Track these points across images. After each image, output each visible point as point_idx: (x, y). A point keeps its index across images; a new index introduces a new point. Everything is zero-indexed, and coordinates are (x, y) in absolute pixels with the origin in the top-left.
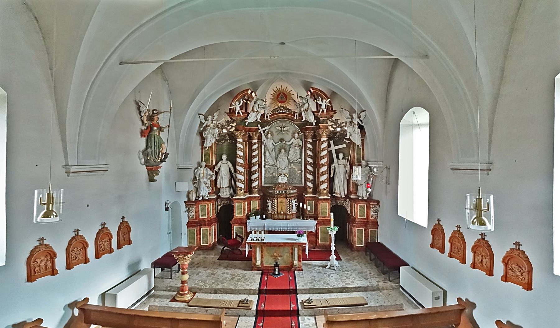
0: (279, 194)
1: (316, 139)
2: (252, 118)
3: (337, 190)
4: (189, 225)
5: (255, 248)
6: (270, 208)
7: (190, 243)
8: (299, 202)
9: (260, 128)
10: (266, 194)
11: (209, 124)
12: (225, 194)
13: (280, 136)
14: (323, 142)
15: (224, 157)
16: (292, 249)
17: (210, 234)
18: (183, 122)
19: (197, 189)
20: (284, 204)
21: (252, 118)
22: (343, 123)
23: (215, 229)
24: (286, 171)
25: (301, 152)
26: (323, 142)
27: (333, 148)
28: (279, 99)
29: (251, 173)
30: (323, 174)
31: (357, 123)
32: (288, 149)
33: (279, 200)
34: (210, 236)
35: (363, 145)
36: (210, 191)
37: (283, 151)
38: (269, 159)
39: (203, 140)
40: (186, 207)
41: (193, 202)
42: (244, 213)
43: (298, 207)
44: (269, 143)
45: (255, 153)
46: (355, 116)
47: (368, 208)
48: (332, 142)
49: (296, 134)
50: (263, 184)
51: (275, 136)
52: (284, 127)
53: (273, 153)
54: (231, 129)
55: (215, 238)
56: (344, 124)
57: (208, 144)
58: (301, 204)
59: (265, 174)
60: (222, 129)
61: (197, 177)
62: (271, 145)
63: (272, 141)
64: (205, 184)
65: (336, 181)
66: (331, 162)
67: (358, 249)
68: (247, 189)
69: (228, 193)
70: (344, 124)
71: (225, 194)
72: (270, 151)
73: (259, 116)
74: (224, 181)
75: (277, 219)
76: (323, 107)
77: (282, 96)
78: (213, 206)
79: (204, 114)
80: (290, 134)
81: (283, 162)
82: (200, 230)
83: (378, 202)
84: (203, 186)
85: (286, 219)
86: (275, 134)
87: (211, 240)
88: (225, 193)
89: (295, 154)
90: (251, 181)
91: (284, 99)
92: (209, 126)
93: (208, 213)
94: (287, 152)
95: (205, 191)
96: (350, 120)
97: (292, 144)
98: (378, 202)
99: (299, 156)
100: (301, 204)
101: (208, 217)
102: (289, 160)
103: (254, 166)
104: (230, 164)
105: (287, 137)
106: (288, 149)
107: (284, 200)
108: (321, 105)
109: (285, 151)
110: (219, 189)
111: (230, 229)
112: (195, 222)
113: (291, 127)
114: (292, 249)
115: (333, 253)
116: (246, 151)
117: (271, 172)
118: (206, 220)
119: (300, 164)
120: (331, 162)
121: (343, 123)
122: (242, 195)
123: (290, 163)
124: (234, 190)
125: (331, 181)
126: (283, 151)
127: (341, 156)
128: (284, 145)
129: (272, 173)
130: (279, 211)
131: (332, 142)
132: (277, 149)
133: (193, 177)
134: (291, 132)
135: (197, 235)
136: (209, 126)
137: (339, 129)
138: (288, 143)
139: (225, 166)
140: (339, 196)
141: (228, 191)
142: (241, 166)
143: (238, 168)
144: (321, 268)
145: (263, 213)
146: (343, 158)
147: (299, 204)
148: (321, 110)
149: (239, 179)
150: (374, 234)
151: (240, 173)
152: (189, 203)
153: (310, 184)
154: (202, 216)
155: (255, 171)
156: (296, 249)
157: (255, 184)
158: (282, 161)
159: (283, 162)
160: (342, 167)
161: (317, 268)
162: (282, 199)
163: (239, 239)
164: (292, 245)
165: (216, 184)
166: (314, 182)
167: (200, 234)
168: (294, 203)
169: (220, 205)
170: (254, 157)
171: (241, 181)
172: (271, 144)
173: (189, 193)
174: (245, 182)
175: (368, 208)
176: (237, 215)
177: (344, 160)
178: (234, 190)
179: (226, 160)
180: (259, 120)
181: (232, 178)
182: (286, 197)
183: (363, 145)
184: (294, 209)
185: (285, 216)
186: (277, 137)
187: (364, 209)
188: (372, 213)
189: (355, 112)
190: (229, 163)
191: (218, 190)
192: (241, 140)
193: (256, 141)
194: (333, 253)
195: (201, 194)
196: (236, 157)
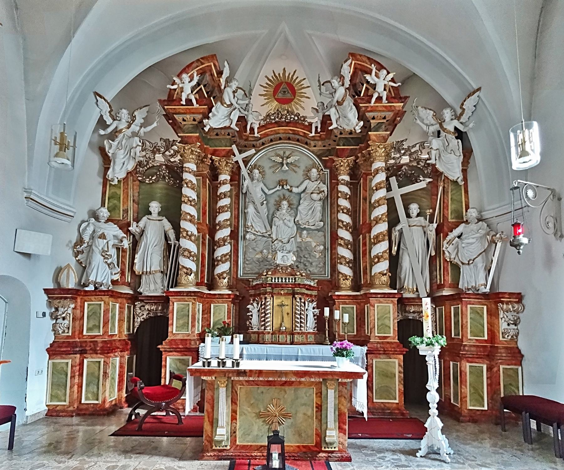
0: (277, 285)
1: (359, 176)
2: (219, 118)
3: (408, 283)
4: (54, 351)
5: (213, 386)
6: (255, 320)
7: (53, 397)
8: (320, 306)
9: (236, 151)
10: (245, 293)
11: (120, 127)
12: (152, 287)
13: (279, 176)
14: (377, 171)
15: (155, 207)
16: (319, 394)
17: (105, 373)
18: (46, 88)
19: (84, 268)
20: (287, 309)
21: (219, 118)
22: (414, 146)
23: (121, 367)
24: (291, 246)
25: (323, 208)
26: (377, 171)
27: (397, 193)
28: (280, 96)
29: (214, 245)
30: (378, 239)
31: (452, 130)
32: (295, 202)
33: (277, 301)
34: (110, 382)
35: (465, 179)
36: (117, 277)
37: (285, 203)
38: (255, 221)
39: (107, 161)
40: (50, 304)
41: (68, 291)
42: (193, 326)
43: (320, 319)
44: (254, 187)
45: (225, 202)
46: (447, 114)
47: (493, 314)
48: (393, 180)
49: (314, 170)
50: (240, 273)
51: (267, 176)
52: (288, 158)
53: (264, 210)
54: (172, 156)
55: (120, 390)
56: (417, 148)
57: (118, 172)
58: (327, 310)
59: (245, 254)
60: (154, 153)
61: (86, 238)
62: (260, 194)
63: (262, 185)
64: (104, 254)
65: (405, 263)
66: (393, 221)
67: (475, 418)
68: (202, 278)
69: (159, 286)
70: (417, 148)
71: (152, 287)
72: (258, 204)
73: (235, 117)
74: (150, 258)
75: (272, 343)
76: (380, 88)
77: (284, 90)
78: (121, 313)
79: (109, 98)
80: (301, 172)
81: (284, 228)
82: (81, 364)
83: (519, 297)
84: (97, 259)
85: (292, 343)
86: (268, 172)
87: (112, 393)
88: (152, 287)
89: (311, 212)
90: (213, 263)
91: (289, 96)
92: (120, 131)
93: (106, 323)
94: (294, 208)
95: (102, 273)
96: (437, 127)
97: (304, 191)
98: (519, 297)
99: (318, 215)
100: (327, 310)
101: (105, 332)
102: (297, 224)
103: (221, 228)
104: (168, 226)
105: (295, 178)
106: (295, 202)
107: (287, 301)
108: (374, 86)
109: (290, 205)
110: (140, 277)
111: (159, 365)
112: (73, 345)
113: (304, 156)
114: (319, 394)
115: (433, 411)
116: (205, 196)
117: (258, 250)
118: (99, 340)
119: (321, 233)
120: (393, 221)
121: (414, 146)
122: (189, 283)
123: (300, 229)
124: (173, 275)
125: (395, 262)
126: (285, 203)
127: (414, 208)
128: (287, 194)
129: (262, 252)
130: (276, 326)
131: (393, 180)
132: (272, 201)
133: (74, 238)
134: (303, 167)
135: (73, 377)
136: (120, 131)
137: (405, 159)
138: (295, 190)
139: (154, 229)
140: (411, 295)
141: (159, 281)
142: (190, 221)
143: (185, 225)
144: (403, 457)
145: (240, 326)
146: (418, 215)
147: (322, 312)
148: (376, 96)
149: (186, 250)
150: (513, 377)
151: (189, 237)
152: (56, 294)
153: (345, 270)
154: (89, 329)
155: (224, 240)
156: (331, 394)
157: (223, 268)
158: (284, 221)
159: (284, 228)
160: (417, 233)
161: (389, 456)
162: (283, 298)
163: (177, 384)
164: (326, 377)
165: (132, 264)
166: (355, 264)
167: (81, 375)
168: (311, 310)
169: (142, 313)
170: (222, 210)
171: (190, 255)
172: (258, 190)
173: (59, 271)
174: (199, 259)
175: (493, 314)
176: (175, 330)
177: (422, 218)
178: (173, 275)
179: (159, 214)
180: (233, 126)
181: (171, 251)
182: (293, 294)
183: (465, 179)
184: (311, 324)
185: (291, 336)
186: (272, 177)
187: (482, 317)
188: (503, 325)
189: (446, 105)
190: (165, 221)
191: (137, 278)
192: (193, 167)
193: (229, 178)
194: (433, 411)
195: (92, 278)
196: (180, 203)
